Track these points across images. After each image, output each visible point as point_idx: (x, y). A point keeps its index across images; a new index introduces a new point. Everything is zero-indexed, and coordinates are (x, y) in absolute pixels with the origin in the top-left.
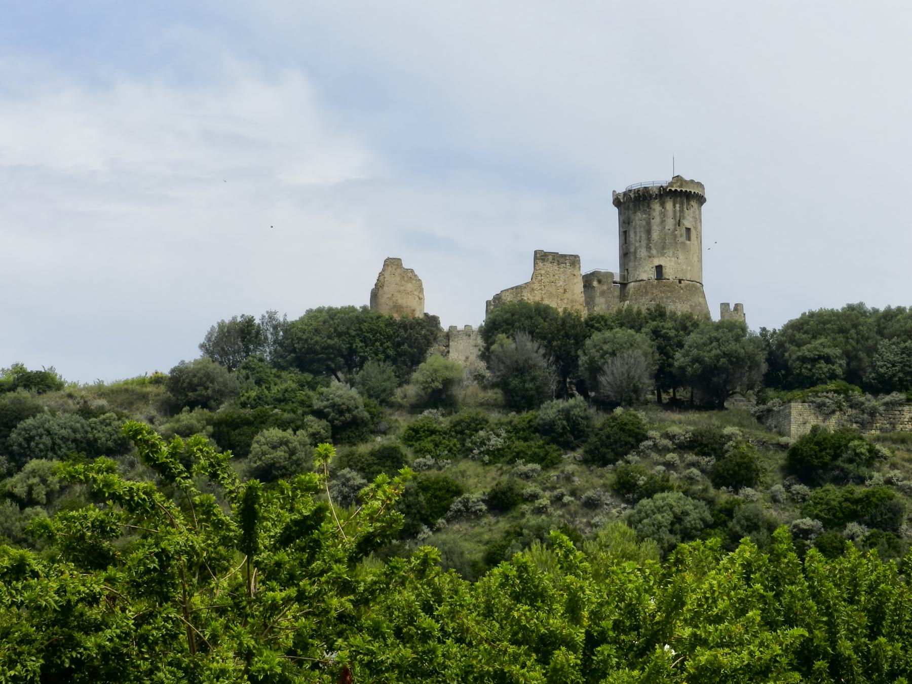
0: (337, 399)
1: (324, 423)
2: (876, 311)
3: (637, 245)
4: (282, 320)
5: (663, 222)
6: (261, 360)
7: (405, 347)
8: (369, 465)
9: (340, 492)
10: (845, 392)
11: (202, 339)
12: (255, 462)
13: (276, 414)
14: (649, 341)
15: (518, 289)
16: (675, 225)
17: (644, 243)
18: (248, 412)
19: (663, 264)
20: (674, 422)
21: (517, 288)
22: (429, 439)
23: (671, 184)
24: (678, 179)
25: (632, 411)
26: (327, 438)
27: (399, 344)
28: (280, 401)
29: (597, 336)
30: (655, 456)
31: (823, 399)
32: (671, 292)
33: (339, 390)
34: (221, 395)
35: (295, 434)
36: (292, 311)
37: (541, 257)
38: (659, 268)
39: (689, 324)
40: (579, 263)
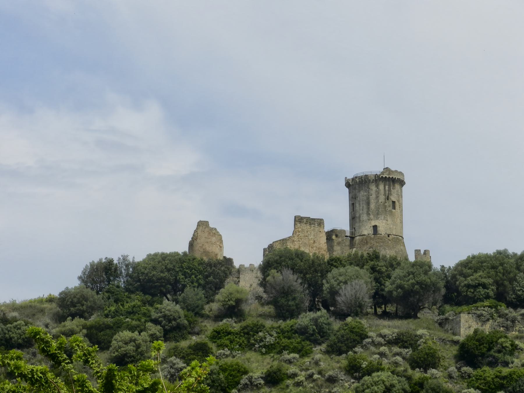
0: (167, 312)
1: (159, 327)
2: (515, 255)
3: (361, 212)
4: (131, 261)
5: (377, 197)
6: (118, 287)
7: (211, 278)
8: (188, 355)
9: (169, 372)
10: (496, 307)
11: (80, 274)
12: (114, 353)
13: (128, 322)
14: (369, 274)
15: (284, 241)
17: (365, 211)
18: (109, 321)
20: (385, 326)
21: (283, 240)
22: (227, 338)
23: (383, 173)
24: (387, 169)
25: (358, 319)
26: (161, 337)
27: (207, 277)
28: (130, 313)
29: (335, 271)
30: (373, 349)
31: (481, 311)
32: (383, 242)
33: (168, 306)
34: (92, 310)
35: (140, 334)
36: (138, 254)
37: (299, 220)
38: (375, 227)
39: (394, 263)
40: (323, 224)
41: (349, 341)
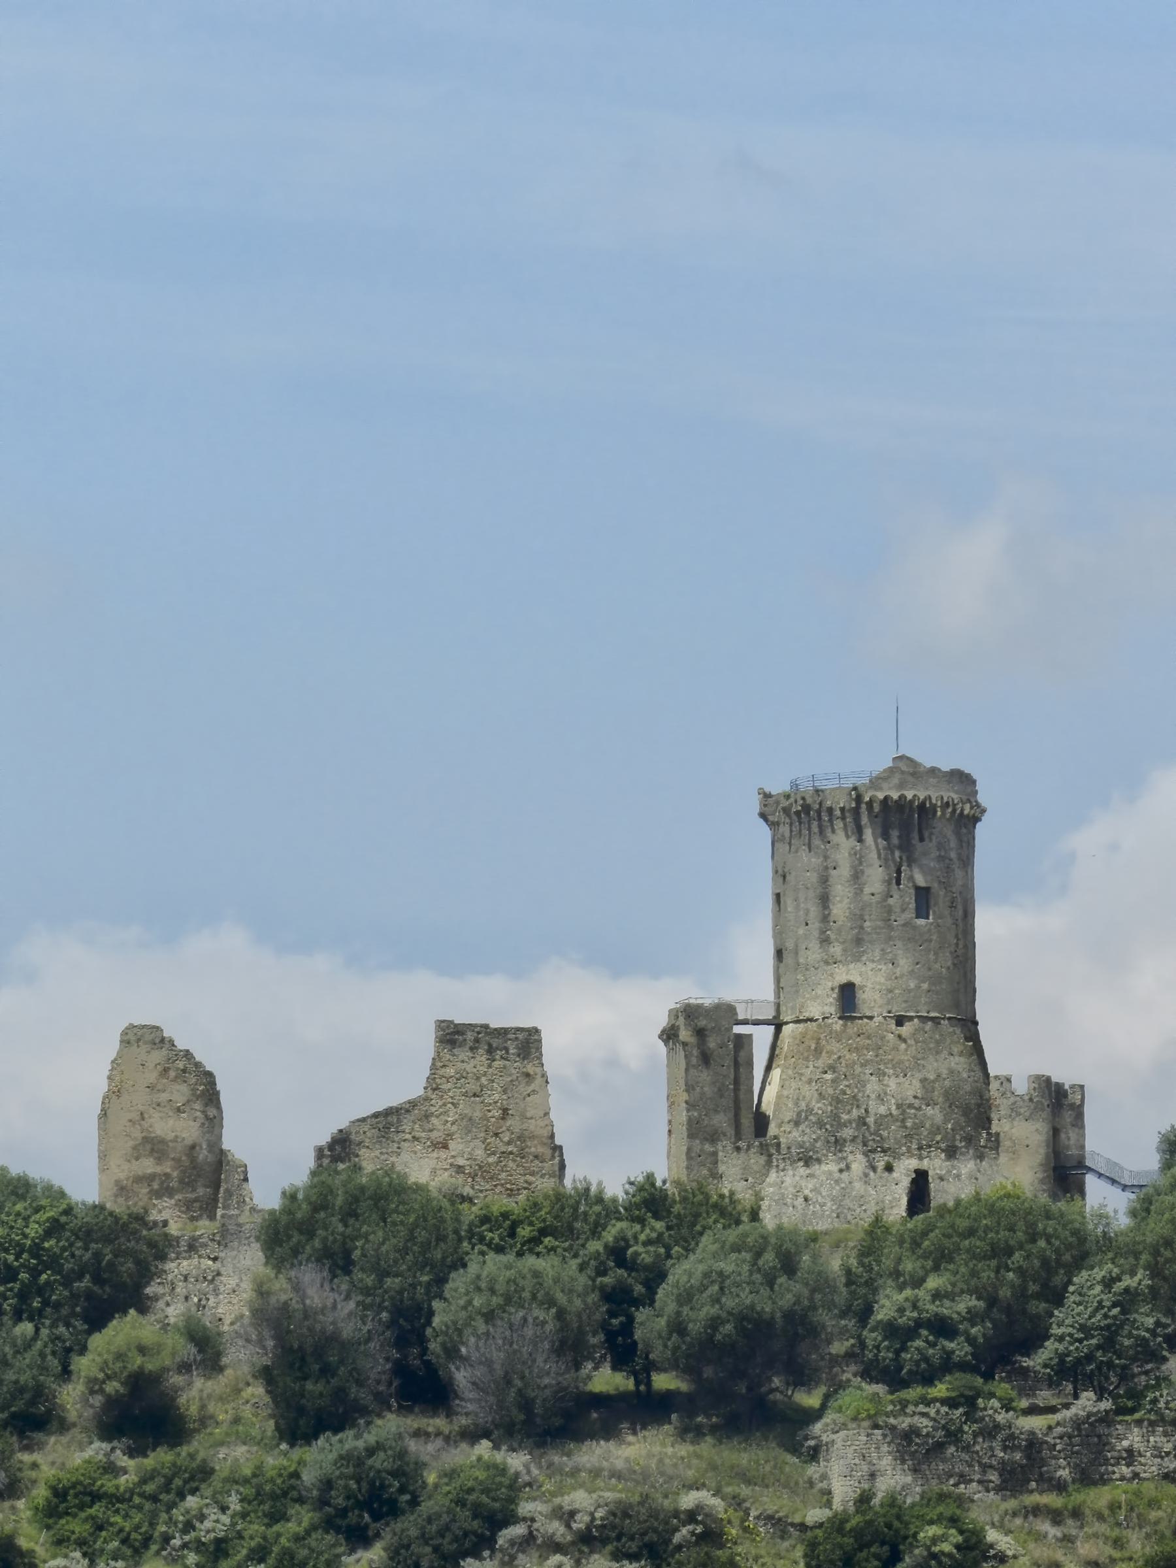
5: (857, 876)
16: (889, 882)
17: (815, 926)
19: (857, 980)
21: (389, 1112)
37: (451, 1036)
40: (539, 1049)
41: (449, 1537)
